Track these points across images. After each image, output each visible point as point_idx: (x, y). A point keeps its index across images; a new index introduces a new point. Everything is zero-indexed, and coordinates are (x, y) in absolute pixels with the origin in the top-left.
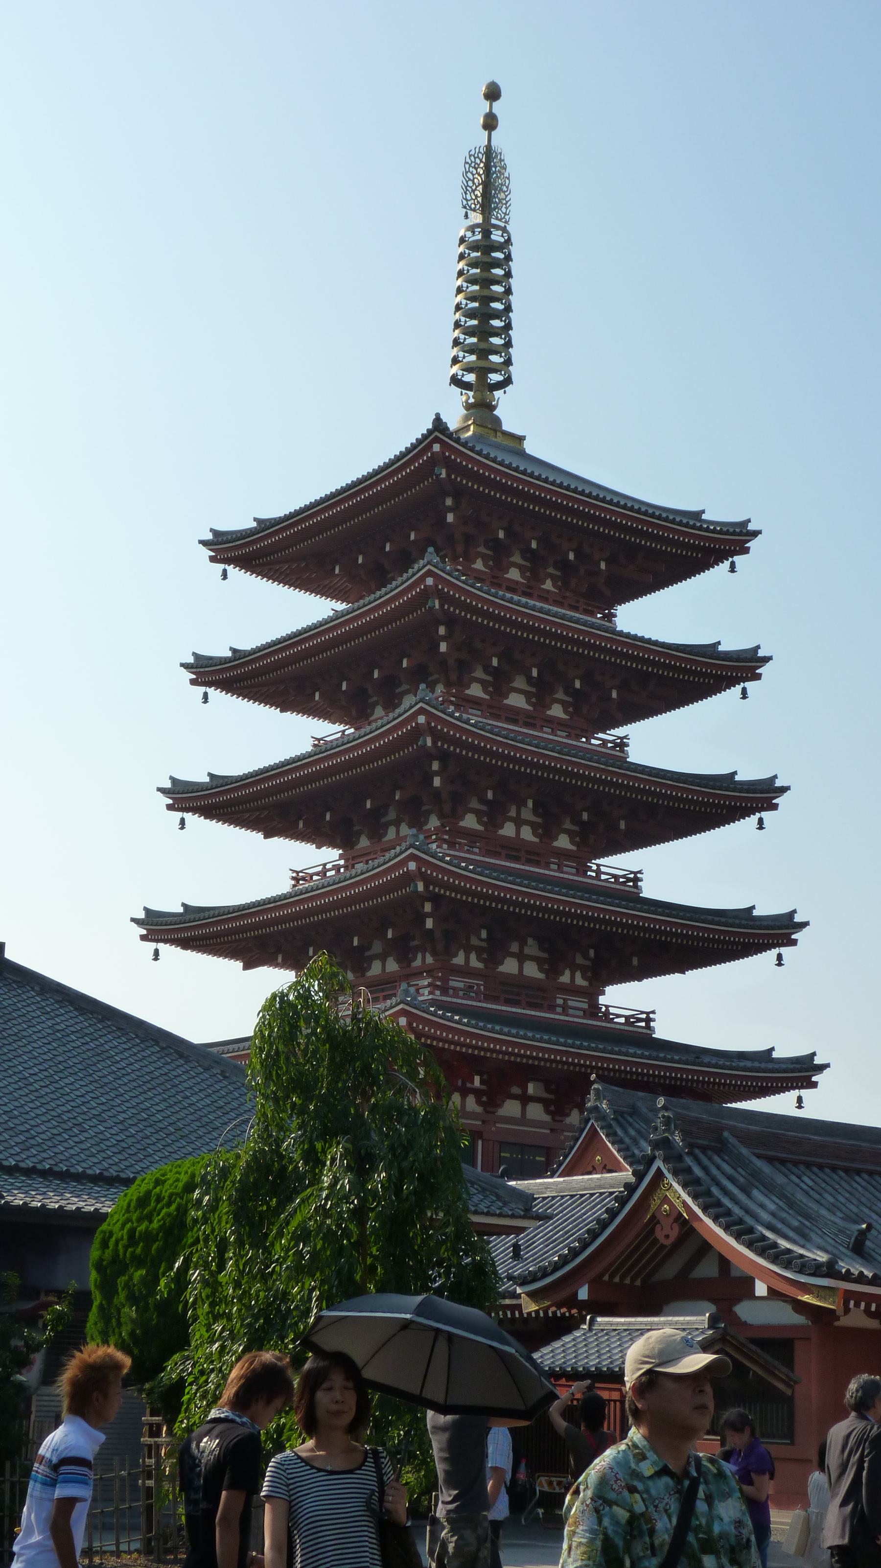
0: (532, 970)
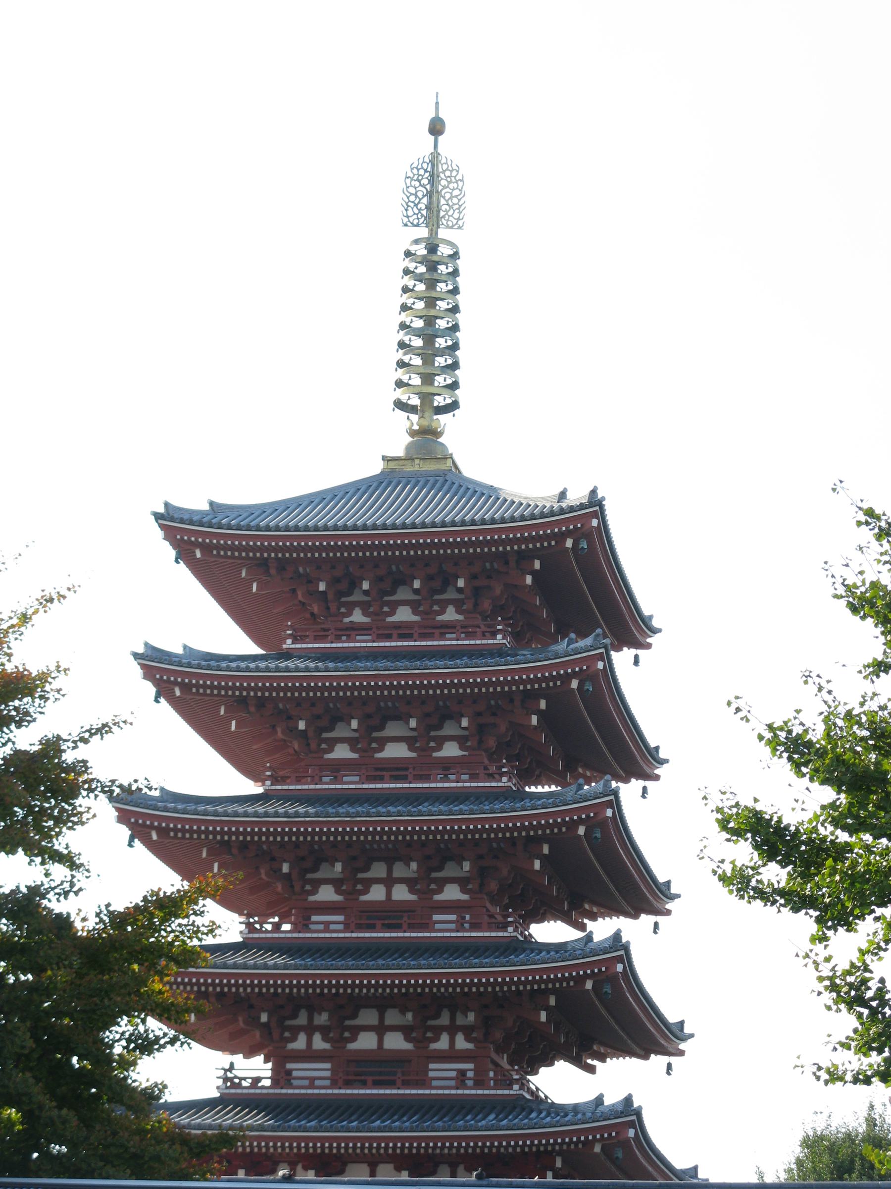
0: (395, 1042)
